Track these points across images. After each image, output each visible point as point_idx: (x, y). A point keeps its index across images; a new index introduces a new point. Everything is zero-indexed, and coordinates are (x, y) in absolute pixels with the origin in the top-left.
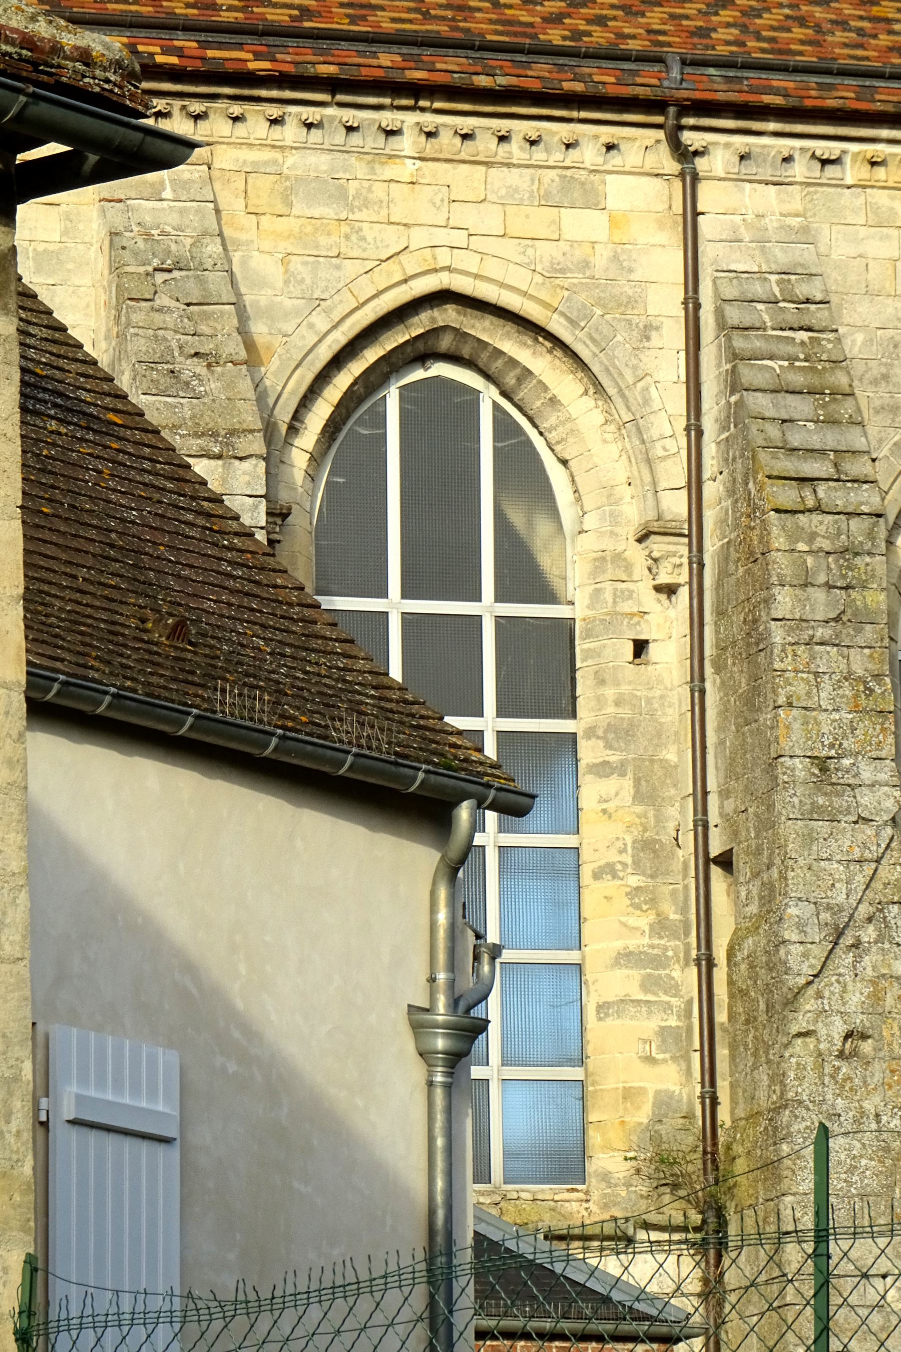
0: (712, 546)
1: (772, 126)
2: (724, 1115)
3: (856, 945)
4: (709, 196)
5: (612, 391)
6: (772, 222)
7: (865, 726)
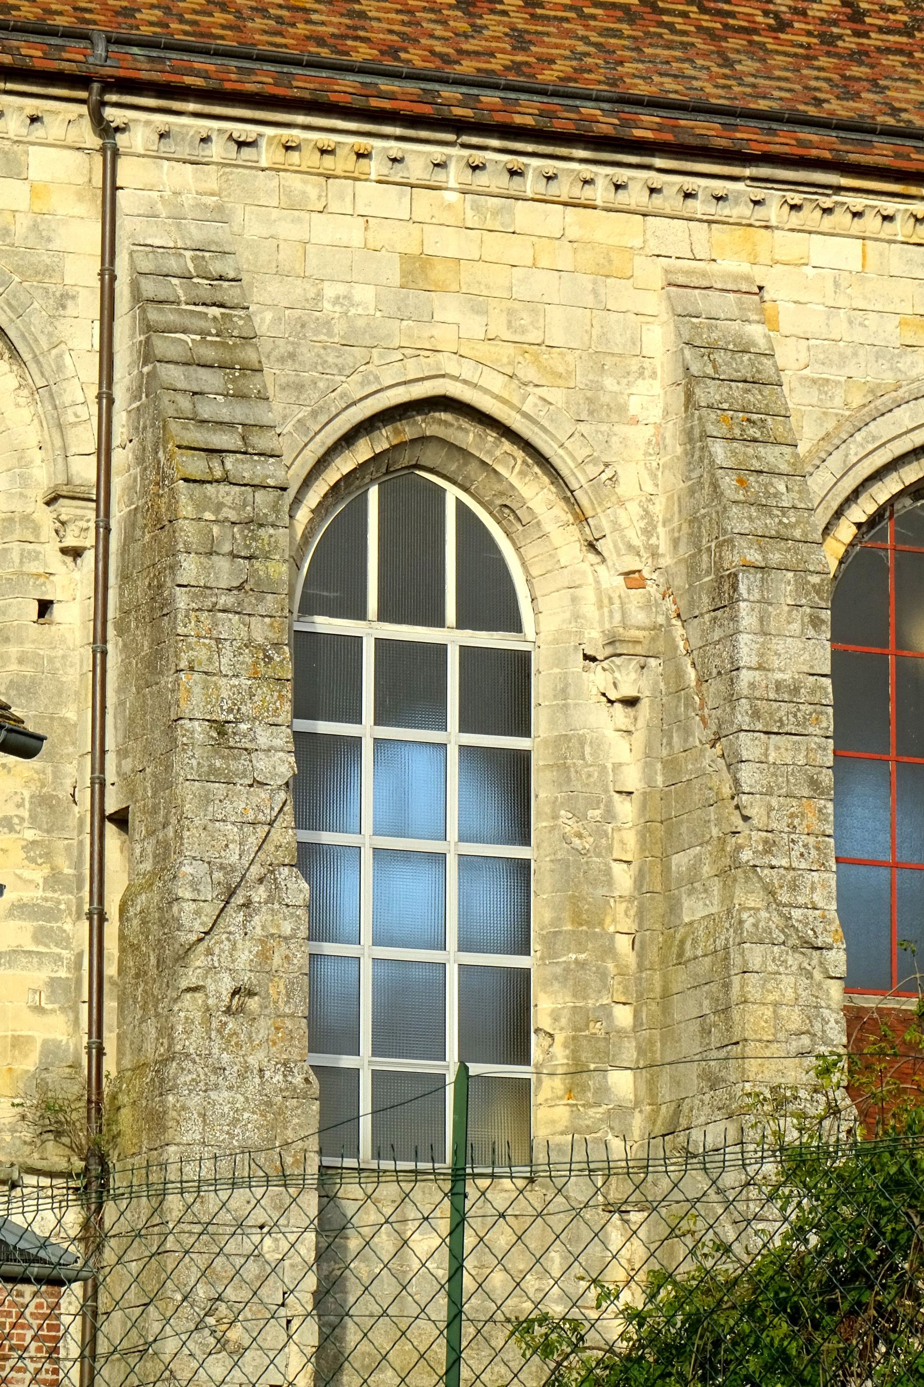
0: (118, 512)
1: (192, 107)
2: (109, 1065)
3: (247, 905)
4: (126, 171)
5: (27, 357)
6: (188, 200)
7: (263, 692)
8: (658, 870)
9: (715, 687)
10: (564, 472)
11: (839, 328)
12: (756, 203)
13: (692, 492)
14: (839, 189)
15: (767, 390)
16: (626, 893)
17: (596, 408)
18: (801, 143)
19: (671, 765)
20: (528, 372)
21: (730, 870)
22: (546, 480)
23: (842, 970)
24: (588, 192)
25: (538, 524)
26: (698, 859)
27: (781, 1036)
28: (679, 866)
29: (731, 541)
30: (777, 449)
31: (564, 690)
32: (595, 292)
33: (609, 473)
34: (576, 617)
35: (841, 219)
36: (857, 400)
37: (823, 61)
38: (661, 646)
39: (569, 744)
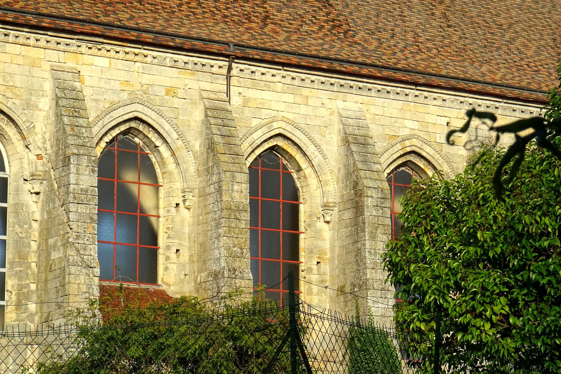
8: (44, 243)
9: (63, 189)
10: (19, 124)
11: (102, 84)
12: (78, 46)
13: (57, 131)
14: (103, 43)
15: (80, 102)
16: (35, 250)
17: (29, 106)
18: (92, 29)
19: (49, 212)
20: (9, 94)
21: (66, 244)
22: (14, 127)
23: (98, 274)
24: (28, 41)
25: (11, 140)
26: (57, 241)
27: (80, 293)
28: (51, 242)
29: (68, 146)
30: (83, 120)
31: (17, 189)
32: (30, 71)
33: (32, 125)
34: (22, 168)
35: (103, 52)
36: (107, 106)
37: (99, 5)
38: (47, 177)
39: (18, 205)
